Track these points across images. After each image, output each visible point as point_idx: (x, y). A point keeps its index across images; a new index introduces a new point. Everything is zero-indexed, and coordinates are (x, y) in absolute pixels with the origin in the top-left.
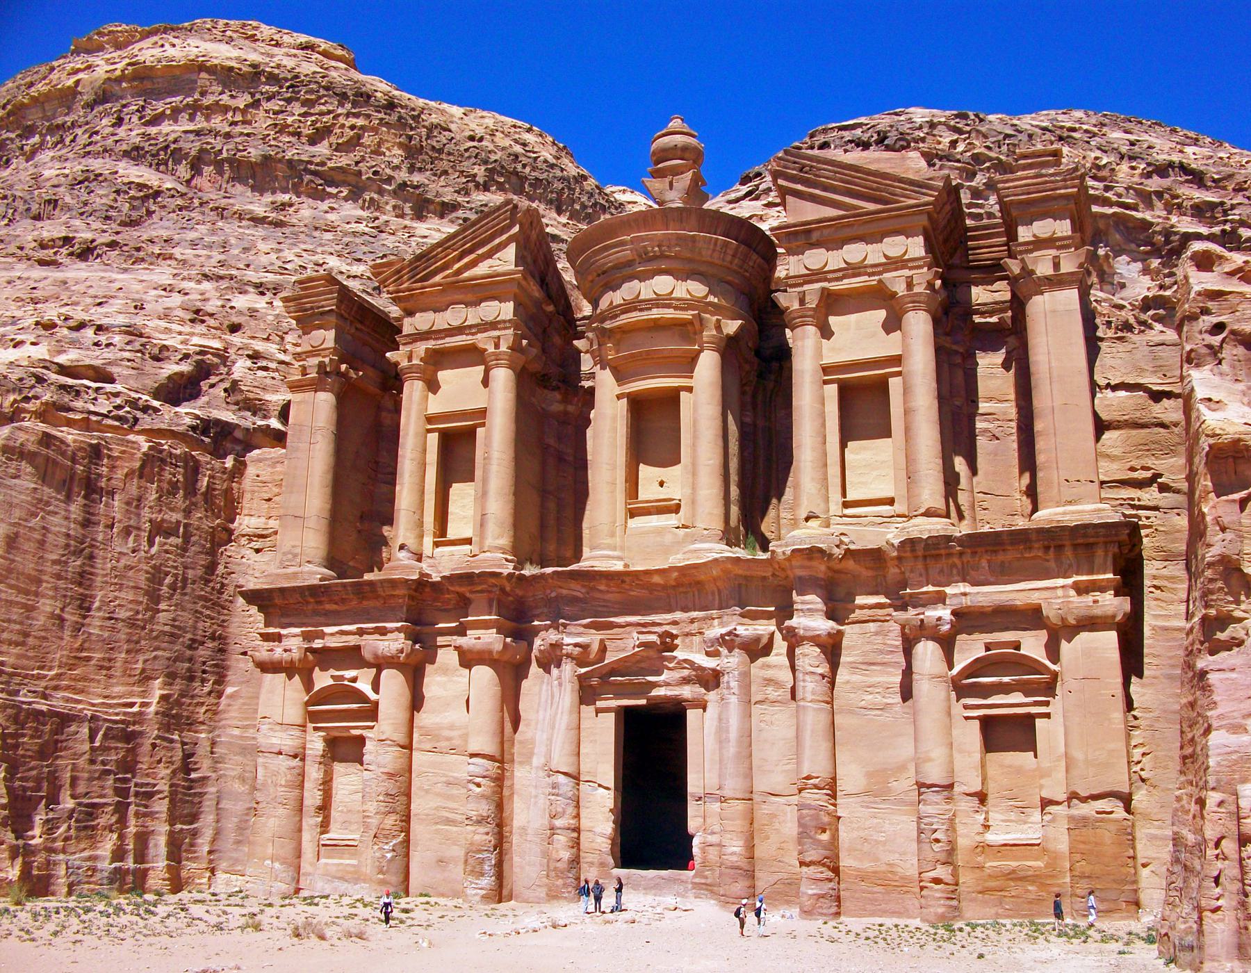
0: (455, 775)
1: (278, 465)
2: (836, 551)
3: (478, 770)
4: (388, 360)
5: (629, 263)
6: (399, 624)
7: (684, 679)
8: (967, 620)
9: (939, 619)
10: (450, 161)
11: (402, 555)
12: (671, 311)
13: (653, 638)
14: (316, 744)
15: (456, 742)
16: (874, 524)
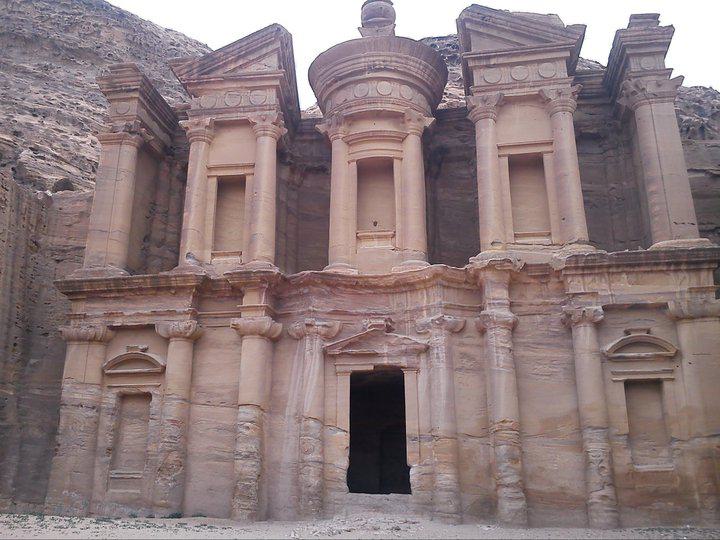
2: (518, 263)
4: (179, 127)
5: (362, 72)
7: (402, 352)
12: (390, 105)
13: (382, 322)
14: (111, 399)
16: (537, 250)
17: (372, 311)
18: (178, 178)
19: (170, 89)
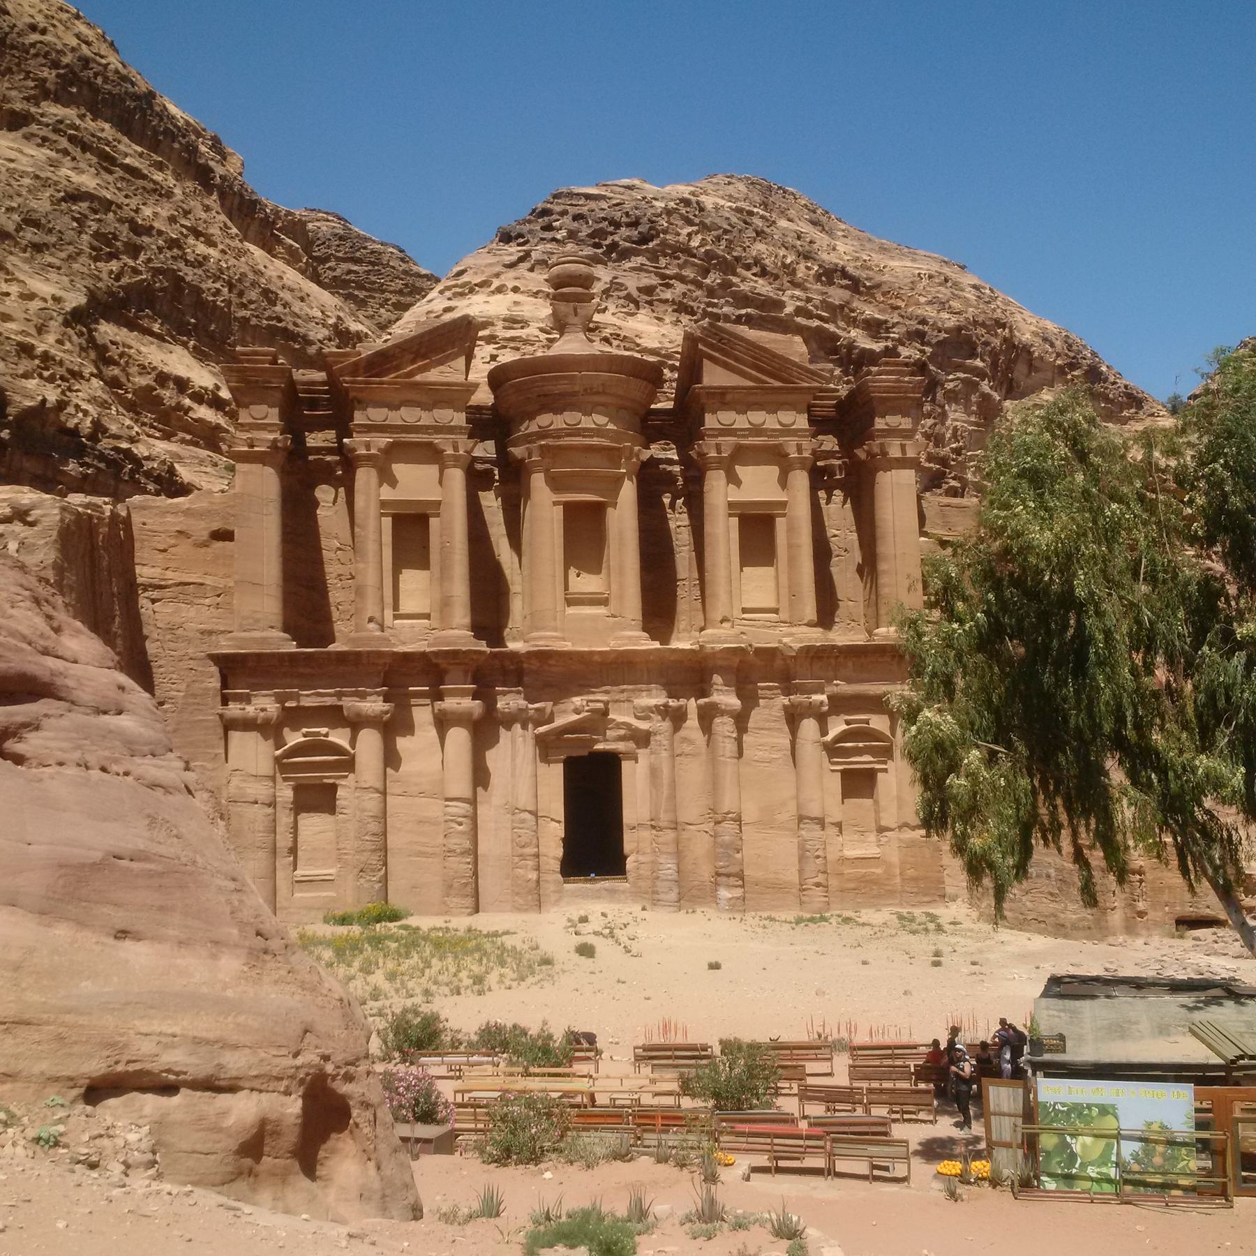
0: (426, 814)
1: (168, 515)
3: (462, 812)
5: (574, 394)
8: (840, 704)
9: (822, 703)
10: (13, 56)
11: (372, 626)
13: (600, 705)
14: (286, 793)
16: (765, 627)
19: (45, 132)
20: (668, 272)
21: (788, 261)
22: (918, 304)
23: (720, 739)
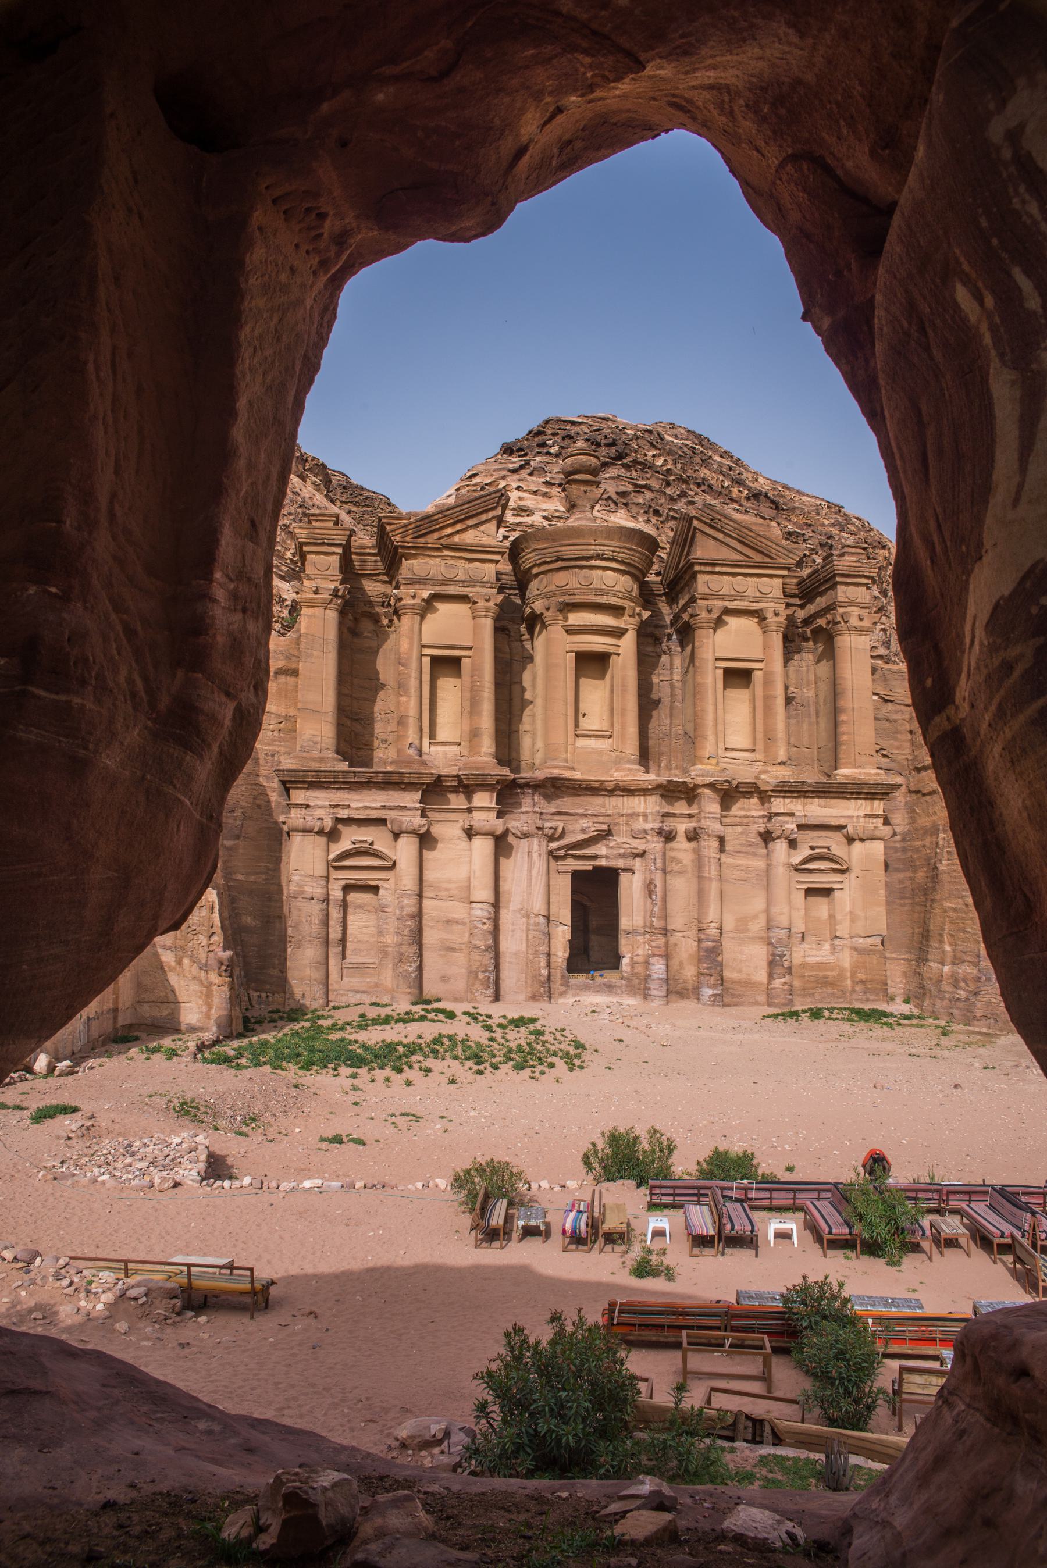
0: (454, 916)
3: (486, 914)
6: (418, 805)
13: (604, 827)
14: (336, 893)
15: (454, 892)
16: (743, 765)
17: (589, 812)
18: (349, 629)
20: (639, 483)
21: (726, 485)
22: (823, 525)
23: (707, 859)
